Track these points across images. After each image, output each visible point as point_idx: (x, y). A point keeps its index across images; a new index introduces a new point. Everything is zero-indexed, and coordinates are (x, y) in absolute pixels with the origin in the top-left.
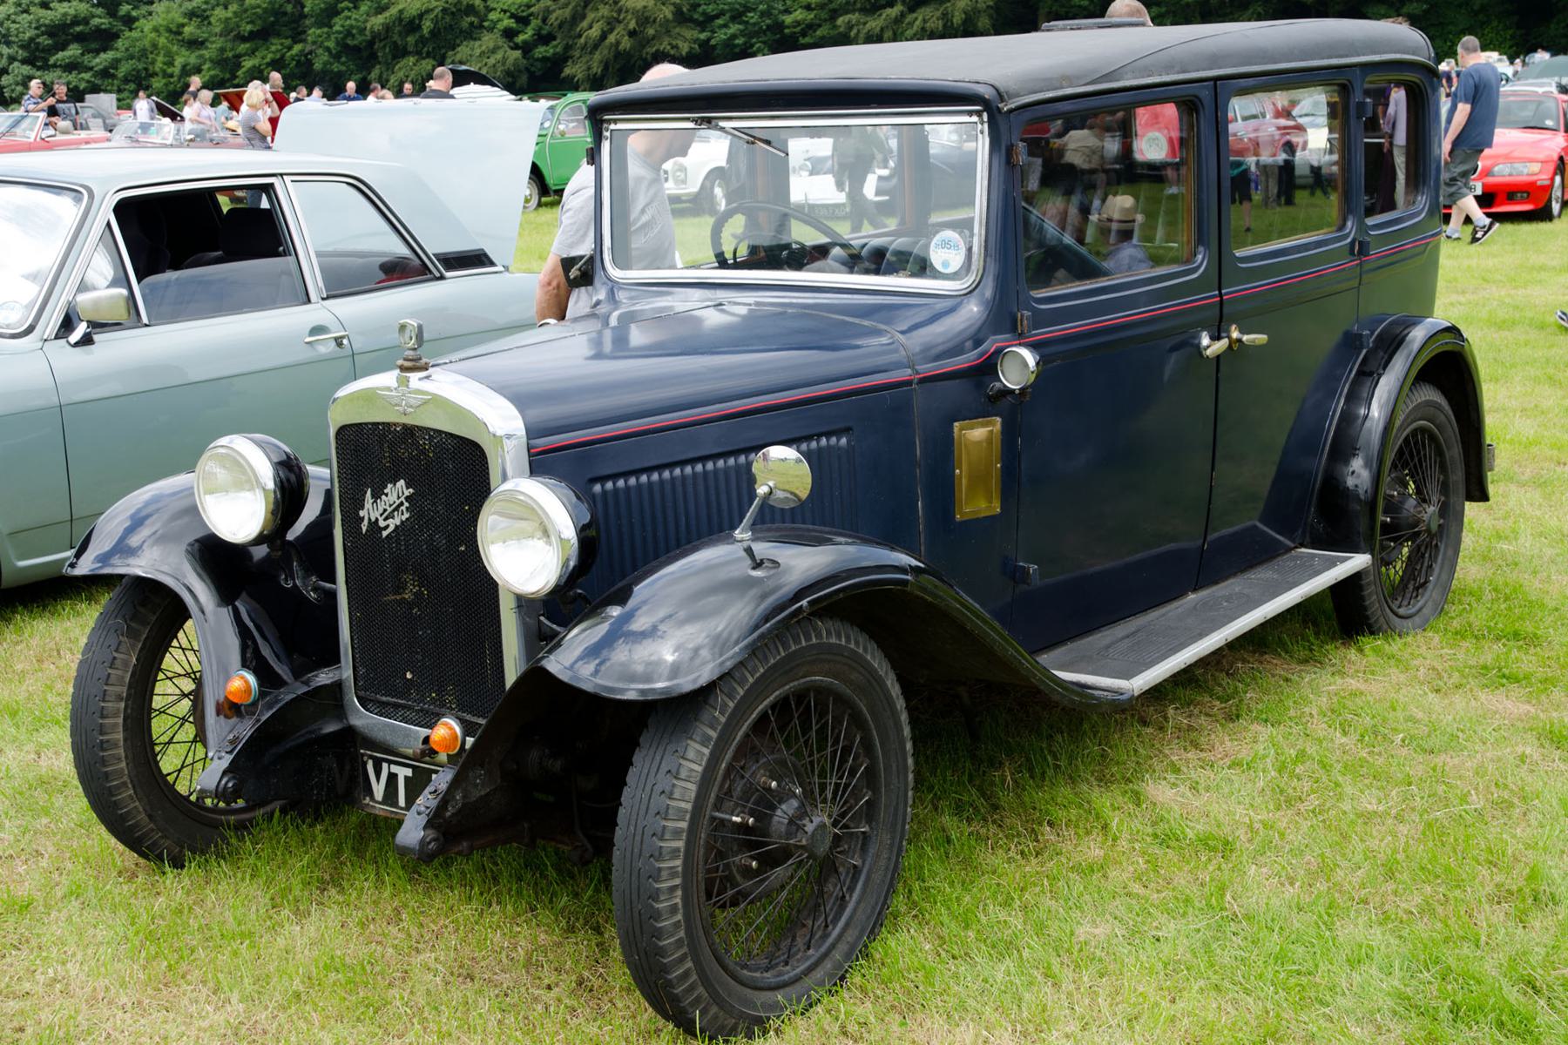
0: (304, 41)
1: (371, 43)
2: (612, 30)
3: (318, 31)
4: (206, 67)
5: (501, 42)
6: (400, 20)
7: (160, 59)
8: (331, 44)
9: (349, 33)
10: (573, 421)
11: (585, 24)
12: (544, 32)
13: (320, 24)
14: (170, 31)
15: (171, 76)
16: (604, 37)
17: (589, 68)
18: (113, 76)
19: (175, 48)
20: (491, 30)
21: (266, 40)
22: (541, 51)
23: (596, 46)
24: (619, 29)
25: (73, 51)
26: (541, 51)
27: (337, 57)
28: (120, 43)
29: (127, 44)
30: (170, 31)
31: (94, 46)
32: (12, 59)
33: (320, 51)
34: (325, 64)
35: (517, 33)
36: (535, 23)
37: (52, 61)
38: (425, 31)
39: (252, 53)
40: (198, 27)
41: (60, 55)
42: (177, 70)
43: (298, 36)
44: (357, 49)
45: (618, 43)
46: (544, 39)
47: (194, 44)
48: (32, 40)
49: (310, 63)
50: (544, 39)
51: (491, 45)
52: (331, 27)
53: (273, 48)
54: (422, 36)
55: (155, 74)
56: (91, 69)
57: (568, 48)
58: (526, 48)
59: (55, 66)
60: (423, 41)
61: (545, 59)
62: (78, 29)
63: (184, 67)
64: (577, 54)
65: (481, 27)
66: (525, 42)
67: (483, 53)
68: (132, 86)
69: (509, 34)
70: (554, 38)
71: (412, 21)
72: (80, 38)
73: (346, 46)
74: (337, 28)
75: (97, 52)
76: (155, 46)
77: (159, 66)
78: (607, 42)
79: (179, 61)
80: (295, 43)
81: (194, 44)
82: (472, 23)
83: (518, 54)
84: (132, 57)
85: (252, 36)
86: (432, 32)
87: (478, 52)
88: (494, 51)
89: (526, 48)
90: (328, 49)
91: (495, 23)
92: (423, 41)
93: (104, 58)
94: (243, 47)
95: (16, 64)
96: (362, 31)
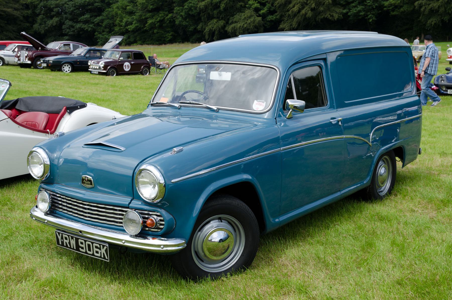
0: (173, 12)
1: (199, 13)
2: (303, 8)
3: (178, 8)
4: (134, 23)
5: (253, 13)
6: (212, 4)
7: (118, 19)
8: (183, 14)
9: (190, 9)
10: (116, 231)
11: (291, 5)
12: (272, 9)
13: (179, 6)
14: (123, 8)
15: (121, 26)
16: (299, 11)
17: (291, 25)
18: (101, 26)
19: (124, 15)
20: (249, 8)
21: (158, 12)
22: (270, 18)
23: (295, 15)
24: (307, 8)
25: (87, 16)
26: (270, 18)
27: (185, 19)
28: (105, 14)
29: (107, 13)
30: (123, 8)
31: (95, 14)
32: (66, 18)
33: (178, 17)
34: (180, 22)
35: (260, 10)
36: (268, 5)
37: (79, 20)
38: (222, 8)
39: (152, 17)
40: (133, 7)
41: (82, 17)
42: (123, 24)
43: (171, 11)
44: (193, 16)
45: (306, 14)
46: (271, 12)
47: (131, 13)
48: (73, 11)
49: (174, 21)
50: (271, 12)
51: (249, 15)
52: (183, 7)
53: (160, 15)
54: (220, 11)
55: (116, 25)
56: (93, 23)
57: (282, 16)
58: (264, 16)
59: (80, 22)
60: (220, 13)
61: (271, 21)
62: (90, 7)
63: (126, 22)
64: (286, 19)
65: (245, 7)
66: (263, 14)
67: (245, 18)
68: (107, 30)
69: (257, 10)
70: (276, 12)
71: (216, 4)
72: (90, 11)
73: (189, 14)
74: (186, 7)
75: (96, 16)
76: (117, 14)
77: (117, 22)
78: (301, 13)
79: (125, 20)
80: (170, 13)
81: (131, 13)
82: (241, 5)
83: (260, 18)
84: (108, 19)
86: (224, 9)
87: (243, 17)
88: (250, 17)
89: (264, 16)
90: (181, 16)
91: (251, 5)
92: (220, 13)
94: (149, 15)
95: (67, 20)
96: (196, 8)
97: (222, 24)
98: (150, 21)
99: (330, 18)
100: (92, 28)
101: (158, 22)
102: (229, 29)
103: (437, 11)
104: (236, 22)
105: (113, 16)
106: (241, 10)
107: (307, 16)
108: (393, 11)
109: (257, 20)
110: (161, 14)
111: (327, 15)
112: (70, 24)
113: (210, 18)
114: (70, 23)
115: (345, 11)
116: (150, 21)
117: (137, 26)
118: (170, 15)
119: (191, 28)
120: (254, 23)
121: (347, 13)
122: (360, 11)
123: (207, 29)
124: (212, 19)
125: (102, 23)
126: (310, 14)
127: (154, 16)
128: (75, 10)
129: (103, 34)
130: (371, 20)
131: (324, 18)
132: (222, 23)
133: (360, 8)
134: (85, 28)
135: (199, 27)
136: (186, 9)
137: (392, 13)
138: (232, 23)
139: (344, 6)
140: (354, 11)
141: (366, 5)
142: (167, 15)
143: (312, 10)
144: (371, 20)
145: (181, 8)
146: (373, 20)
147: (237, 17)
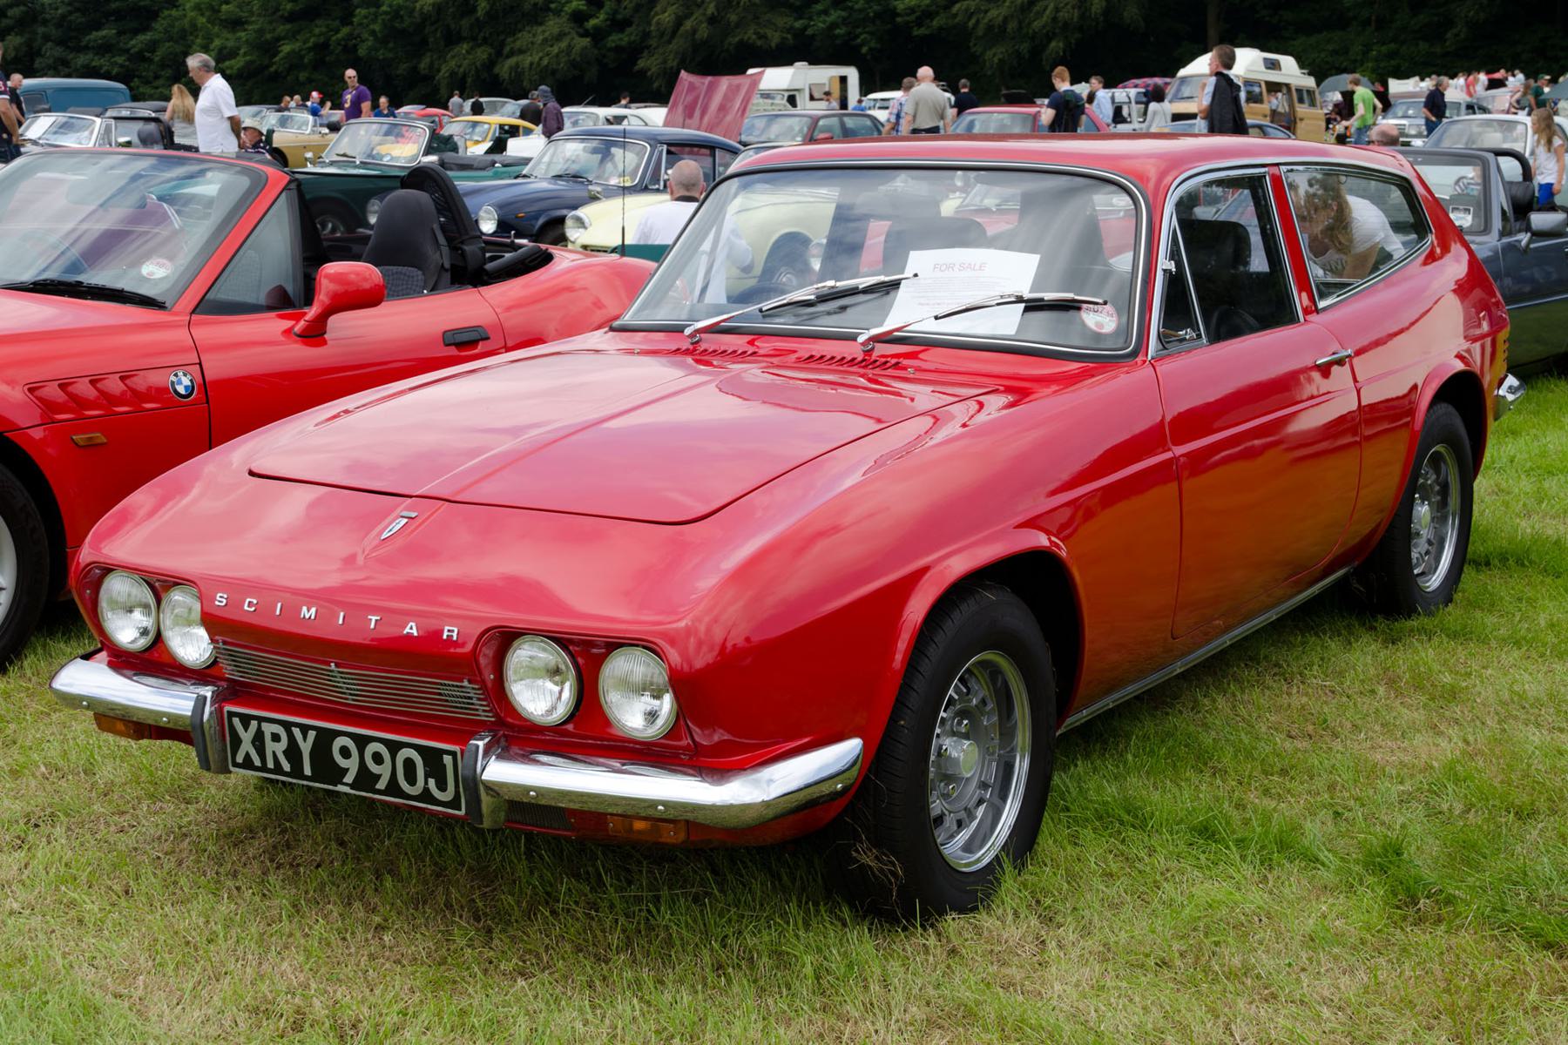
8: (377, 27)
12: (619, 17)
18: (150, 60)
20: (558, 13)
22: (614, 39)
25: (107, 32)
26: (614, 39)
28: (160, 25)
32: (47, 38)
38: (480, 13)
39: (292, 36)
41: (94, 35)
43: (346, 19)
46: (619, 24)
50: (619, 24)
51: (556, 30)
52: (378, 7)
53: (317, 31)
58: (597, 36)
59: (87, 48)
64: (653, 42)
66: (596, 28)
67: (545, 40)
75: (136, 32)
83: (586, 41)
84: (170, 39)
85: (291, 18)
86: (488, 13)
88: (560, 37)
89: (597, 36)
90: (373, 33)
93: (138, 42)
94: (282, 29)
97: (485, 56)
98: (286, 48)
99: (759, 43)
100: (122, 66)
101: (310, 49)
102: (504, 69)
103: (1003, 28)
104: (521, 52)
105: (184, 30)
106: (536, 17)
107: (698, 36)
108: (919, 23)
109: (577, 49)
110: (319, 28)
111: (749, 35)
112: (57, 54)
113: (452, 39)
114: (58, 52)
115: (798, 24)
116: (286, 48)
117: (252, 62)
118: (345, 30)
119: (402, 69)
120: (568, 54)
121: (805, 28)
122: (834, 26)
123: (444, 71)
124: (457, 43)
125: (153, 52)
126: (704, 32)
127: (299, 32)
128: (70, 13)
129: (156, 83)
130: (864, 50)
131: (741, 42)
132: (482, 54)
133: (835, 15)
134: (101, 67)
135: (423, 65)
136: (385, 13)
137: (917, 32)
138: (512, 54)
139: (799, 12)
140: (820, 24)
141: (851, 8)
142: (337, 31)
143: (712, 20)
144: (864, 50)
145: (372, 10)
146: (871, 49)
147: (523, 38)
